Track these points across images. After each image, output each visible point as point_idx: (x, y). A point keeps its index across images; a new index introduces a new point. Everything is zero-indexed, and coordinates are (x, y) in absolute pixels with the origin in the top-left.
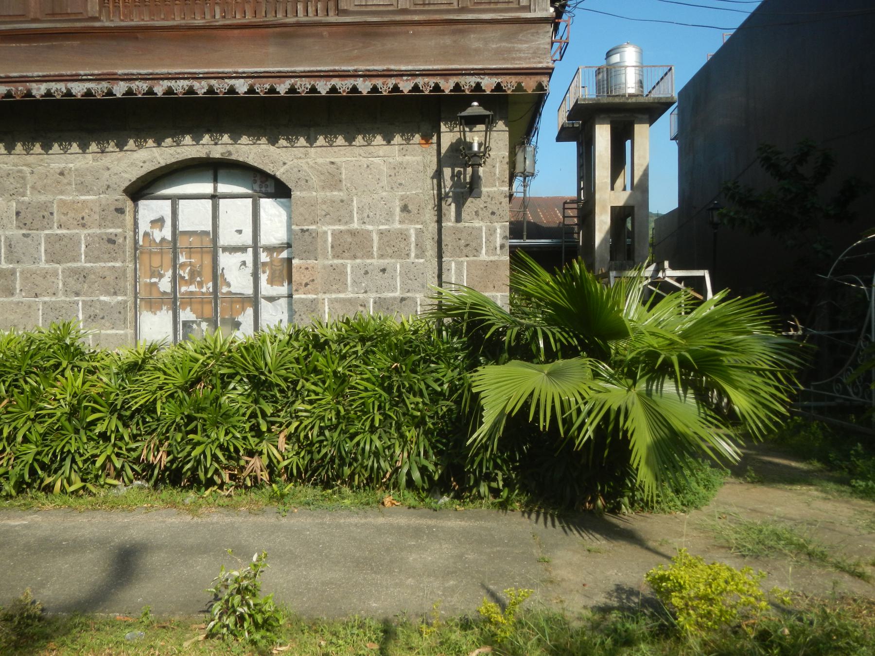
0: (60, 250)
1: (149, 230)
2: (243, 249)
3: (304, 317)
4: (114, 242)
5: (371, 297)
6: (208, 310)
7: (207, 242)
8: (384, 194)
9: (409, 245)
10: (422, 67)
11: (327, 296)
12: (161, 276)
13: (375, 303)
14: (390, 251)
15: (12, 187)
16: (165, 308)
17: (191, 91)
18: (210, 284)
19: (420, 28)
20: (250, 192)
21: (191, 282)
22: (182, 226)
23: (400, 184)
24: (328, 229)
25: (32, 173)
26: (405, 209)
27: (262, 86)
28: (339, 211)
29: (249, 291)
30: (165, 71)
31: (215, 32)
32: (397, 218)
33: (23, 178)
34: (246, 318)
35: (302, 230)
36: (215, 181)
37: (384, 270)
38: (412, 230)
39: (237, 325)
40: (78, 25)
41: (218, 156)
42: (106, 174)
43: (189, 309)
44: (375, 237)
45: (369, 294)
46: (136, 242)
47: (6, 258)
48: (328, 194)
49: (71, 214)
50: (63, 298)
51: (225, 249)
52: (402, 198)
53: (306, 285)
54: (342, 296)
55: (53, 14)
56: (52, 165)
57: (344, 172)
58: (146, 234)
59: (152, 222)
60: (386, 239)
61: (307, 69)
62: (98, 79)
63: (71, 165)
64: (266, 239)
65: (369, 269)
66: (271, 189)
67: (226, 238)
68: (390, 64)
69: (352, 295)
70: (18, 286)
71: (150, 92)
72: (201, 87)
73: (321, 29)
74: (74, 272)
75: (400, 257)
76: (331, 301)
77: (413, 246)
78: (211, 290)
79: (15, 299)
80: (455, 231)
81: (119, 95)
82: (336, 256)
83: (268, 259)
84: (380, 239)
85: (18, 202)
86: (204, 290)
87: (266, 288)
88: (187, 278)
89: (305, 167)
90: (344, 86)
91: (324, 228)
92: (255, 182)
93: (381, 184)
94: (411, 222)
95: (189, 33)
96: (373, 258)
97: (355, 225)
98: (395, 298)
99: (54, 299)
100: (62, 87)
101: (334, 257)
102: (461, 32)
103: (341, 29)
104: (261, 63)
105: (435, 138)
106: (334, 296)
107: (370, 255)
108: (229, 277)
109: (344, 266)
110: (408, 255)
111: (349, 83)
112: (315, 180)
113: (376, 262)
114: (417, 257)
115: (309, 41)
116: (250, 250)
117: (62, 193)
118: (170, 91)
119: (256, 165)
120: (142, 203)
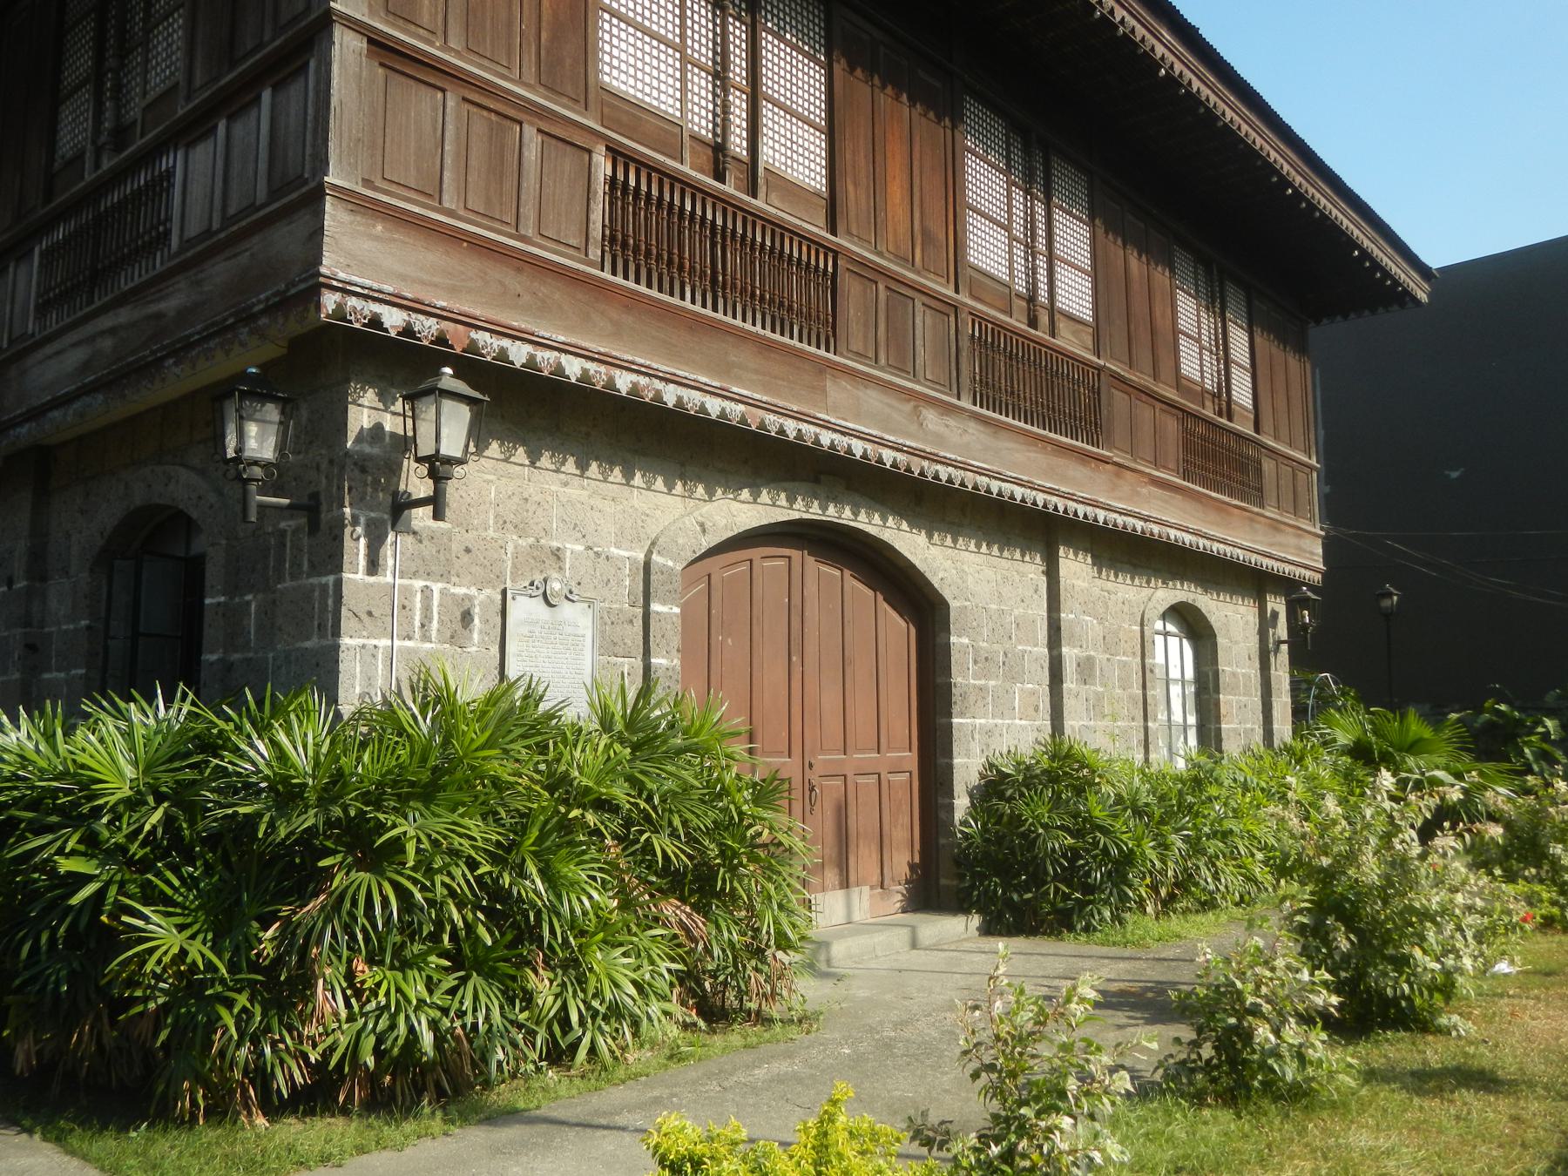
29: (1181, 721)
102: (1299, 536)
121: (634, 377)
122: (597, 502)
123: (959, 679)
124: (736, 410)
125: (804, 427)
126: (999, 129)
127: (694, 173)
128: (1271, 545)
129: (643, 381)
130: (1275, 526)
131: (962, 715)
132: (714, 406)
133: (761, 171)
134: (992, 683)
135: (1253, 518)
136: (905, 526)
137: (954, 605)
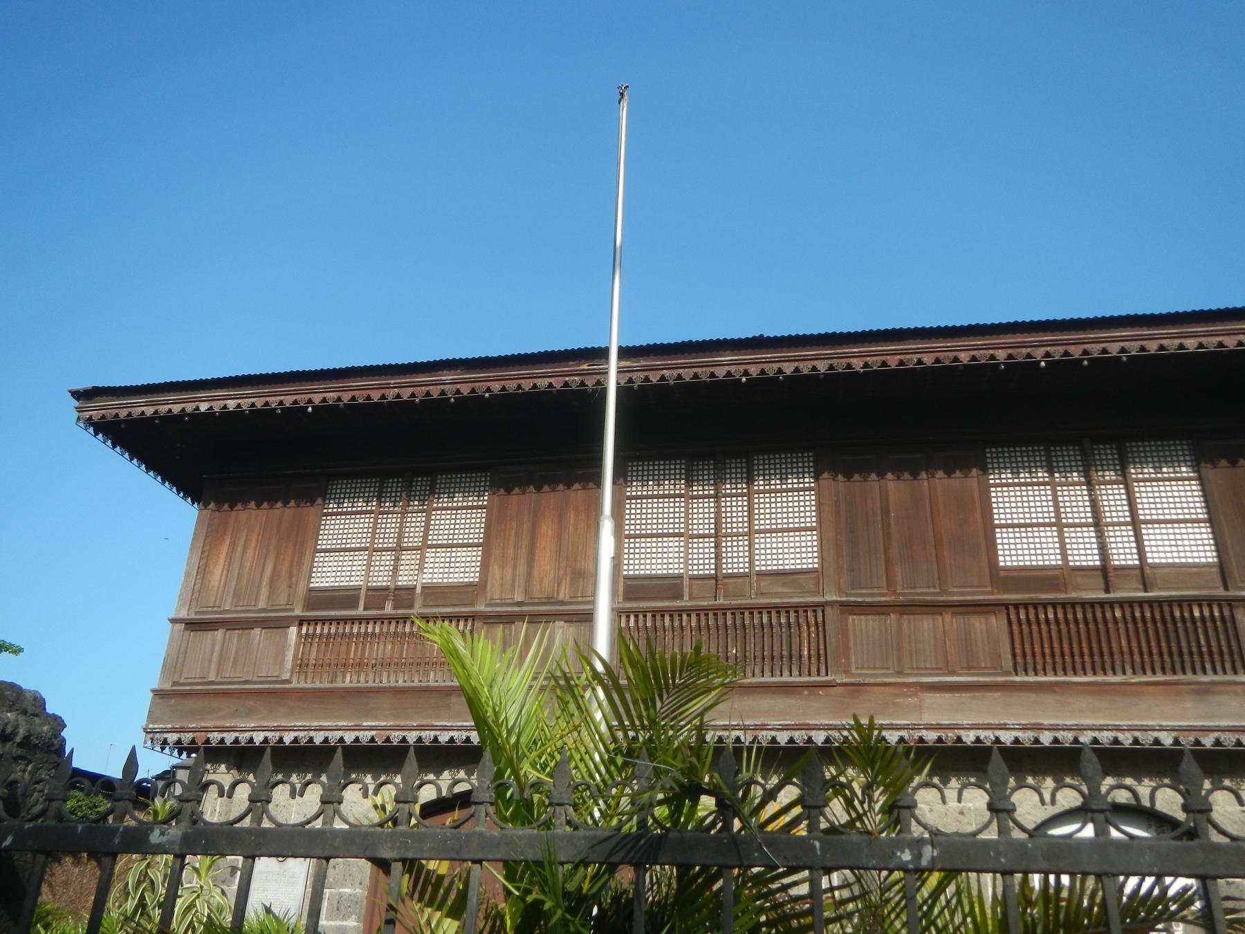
17: (1116, 741)
25: (931, 810)
31: (1128, 687)
40: (1000, 679)
55: (969, 668)
62: (1025, 728)
63: (970, 805)
72: (1126, 739)
92: (1150, 826)
104: (1183, 718)
115: (1224, 698)
119: (1164, 811)
121: (296, 734)
124: (365, 736)
125: (424, 734)
126: (679, 466)
127: (366, 613)
129: (301, 734)
133: (419, 590)
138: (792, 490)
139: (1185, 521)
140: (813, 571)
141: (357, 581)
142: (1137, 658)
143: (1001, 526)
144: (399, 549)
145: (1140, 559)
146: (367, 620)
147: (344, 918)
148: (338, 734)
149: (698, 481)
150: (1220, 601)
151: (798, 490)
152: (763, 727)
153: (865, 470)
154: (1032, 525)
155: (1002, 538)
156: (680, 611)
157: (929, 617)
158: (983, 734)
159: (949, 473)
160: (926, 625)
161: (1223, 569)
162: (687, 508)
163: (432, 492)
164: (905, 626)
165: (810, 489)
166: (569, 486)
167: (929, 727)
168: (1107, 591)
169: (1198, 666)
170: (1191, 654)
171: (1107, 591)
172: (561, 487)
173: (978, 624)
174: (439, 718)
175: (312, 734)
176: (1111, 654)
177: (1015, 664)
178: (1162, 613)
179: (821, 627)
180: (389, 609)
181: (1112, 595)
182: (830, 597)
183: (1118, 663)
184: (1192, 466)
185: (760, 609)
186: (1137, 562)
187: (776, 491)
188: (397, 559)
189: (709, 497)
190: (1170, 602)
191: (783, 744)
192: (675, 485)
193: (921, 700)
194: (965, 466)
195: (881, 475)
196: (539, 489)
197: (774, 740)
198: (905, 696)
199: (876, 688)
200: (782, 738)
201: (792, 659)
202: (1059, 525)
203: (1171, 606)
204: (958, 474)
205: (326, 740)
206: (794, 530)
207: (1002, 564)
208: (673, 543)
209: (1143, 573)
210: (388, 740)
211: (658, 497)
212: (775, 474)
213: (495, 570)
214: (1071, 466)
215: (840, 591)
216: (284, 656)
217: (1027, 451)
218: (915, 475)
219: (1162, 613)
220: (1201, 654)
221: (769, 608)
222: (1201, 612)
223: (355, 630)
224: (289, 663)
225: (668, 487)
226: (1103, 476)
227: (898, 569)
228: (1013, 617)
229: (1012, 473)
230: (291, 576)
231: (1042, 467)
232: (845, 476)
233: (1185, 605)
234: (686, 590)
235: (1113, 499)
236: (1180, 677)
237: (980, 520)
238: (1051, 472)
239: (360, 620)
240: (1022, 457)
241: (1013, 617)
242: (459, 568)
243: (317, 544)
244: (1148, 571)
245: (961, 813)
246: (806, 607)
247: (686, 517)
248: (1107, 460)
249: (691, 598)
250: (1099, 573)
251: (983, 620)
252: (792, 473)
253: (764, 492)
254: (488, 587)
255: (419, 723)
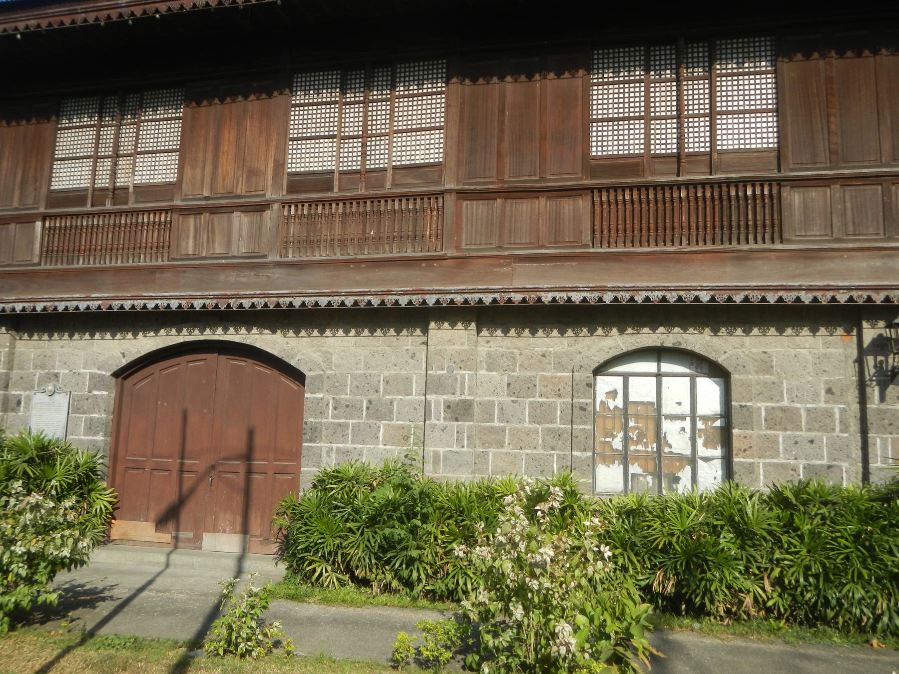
0: (541, 414)
1: (604, 399)
2: (682, 418)
3: (743, 477)
4: (585, 410)
5: (801, 464)
6: (651, 465)
7: (651, 411)
8: (810, 378)
9: (834, 421)
10: (857, 284)
11: (761, 461)
12: (614, 437)
13: (805, 468)
14: (817, 426)
15: (505, 364)
16: (616, 462)
17: (664, 299)
18: (655, 445)
19: (853, 253)
20: (687, 371)
21: (637, 443)
22: (632, 398)
23: (825, 371)
24: (763, 406)
25: (521, 354)
26: (829, 391)
27: (721, 298)
28: (771, 391)
29: (688, 452)
30: (644, 284)
32: (823, 399)
33: (514, 358)
34: (685, 474)
35: (741, 406)
36: (659, 361)
37: (812, 442)
38: (836, 409)
39: (677, 480)
40: (578, 251)
41: (670, 345)
42: (579, 357)
43: (636, 464)
44: (803, 414)
45: (800, 461)
46: (595, 408)
47: (499, 418)
48: (761, 377)
49: (550, 387)
50: (542, 451)
51: (668, 417)
52: (826, 383)
53: (745, 450)
54: (775, 461)
55: (555, 242)
56: (536, 349)
57: (775, 360)
58: (602, 403)
59: (607, 393)
60: (813, 416)
61: (760, 284)
62: (592, 290)
64: (701, 410)
65: (798, 439)
66: (706, 370)
67: (668, 408)
68: (829, 280)
69: (783, 461)
70: (507, 440)
71: (632, 299)
72: (672, 297)
73: (769, 254)
74: (550, 431)
75: (826, 431)
76: (765, 465)
77: (837, 422)
78: (655, 449)
79: (504, 450)
80: (880, 412)
81: (608, 303)
82: (769, 428)
83: (703, 427)
84: (808, 415)
85: (509, 376)
86: (649, 449)
87: (702, 451)
88: (635, 439)
89: (742, 355)
90: (789, 297)
91: (759, 405)
93: (807, 371)
94: (835, 402)
95: (663, 256)
96: (801, 430)
97: (786, 403)
98: (822, 466)
99: (534, 452)
100: (564, 295)
101: (767, 428)
102: (889, 256)
103: (787, 254)
104: (720, 279)
105: (855, 332)
106: (768, 461)
107: (799, 428)
108: (670, 439)
109: (777, 436)
110: (833, 430)
111: (793, 295)
112: (751, 367)
113: (804, 434)
114: (841, 431)
115: (759, 263)
116: (688, 419)
117: (543, 370)
118: (647, 299)
120: (598, 378)
121: (45, 304)
122: (76, 352)
123: (311, 420)
124: (94, 305)
125: (136, 303)
126: (335, 77)
128: (794, 277)
129: (49, 304)
130: (807, 255)
131: (311, 441)
132: (82, 306)
133: (131, 189)
134: (351, 421)
135: (742, 257)
136: (267, 331)
137: (308, 374)
138: (427, 94)
139: (755, 111)
140: (438, 164)
141: (85, 183)
142: (694, 232)
143: (597, 121)
144: (116, 156)
145: (711, 147)
146: (93, 215)
147: (95, 434)
148: (75, 304)
149: (351, 89)
150: (770, 181)
151: (431, 94)
152: (389, 293)
153: (488, 74)
154: (624, 119)
155: (596, 131)
156: (330, 201)
157: (529, 200)
158: (558, 295)
159: (559, 75)
160: (524, 208)
161: (779, 153)
162: (340, 113)
163: (141, 108)
164: (508, 208)
165: (441, 93)
166: (246, 97)
167: (517, 291)
168: (678, 175)
169: (742, 237)
170: (739, 227)
171: (678, 175)
172: (240, 98)
173: (567, 205)
174: (146, 290)
175: (56, 304)
176: (673, 229)
177: (593, 238)
178: (720, 192)
179: (441, 210)
180: (108, 206)
181: (679, 179)
182: (449, 186)
183: (677, 237)
184: (771, 61)
185: (393, 197)
186: (708, 149)
187: (413, 96)
188: (115, 164)
189: (359, 103)
190: (729, 183)
191: (403, 306)
192: (331, 93)
193: (514, 269)
194: (573, 68)
195: (502, 78)
196: (222, 101)
197: (397, 302)
198: (502, 266)
199: (479, 261)
200: (403, 301)
201: (416, 237)
202: (647, 118)
203: (728, 187)
204: (567, 75)
205: (66, 308)
206: (426, 129)
207: (594, 154)
208: (327, 144)
209: (710, 159)
210: (110, 307)
211: (317, 104)
212: (414, 81)
213: (188, 171)
214: (666, 64)
215: (458, 181)
216: (33, 244)
217: (629, 52)
218: (530, 77)
219: (720, 192)
220: (747, 227)
221: (400, 197)
222: (754, 191)
223: (85, 223)
224: (37, 251)
225: (325, 96)
226: (693, 73)
227: (507, 160)
228: (597, 199)
229: (613, 72)
230: (36, 181)
231: (640, 66)
232: (471, 81)
233: (741, 186)
234: (336, 184)
235: (697, 94)
236: (727, 246)
237: (579, 116)
238: (647, 71)
239: (88, 215)
240: (624, 57)
241: (597, 199)
242: (159, 170)
243: (54, 154)
244: (715, 156)
245: (544, 356)
246: (429, 195)
247: (340, 122)
248: (698, 57)
249: (340, 190)
250: (675, 159)
251: (571, 202)
252: (428, 79)
253: (403, 97)
254: (184, 186)
255: (132, 294)
